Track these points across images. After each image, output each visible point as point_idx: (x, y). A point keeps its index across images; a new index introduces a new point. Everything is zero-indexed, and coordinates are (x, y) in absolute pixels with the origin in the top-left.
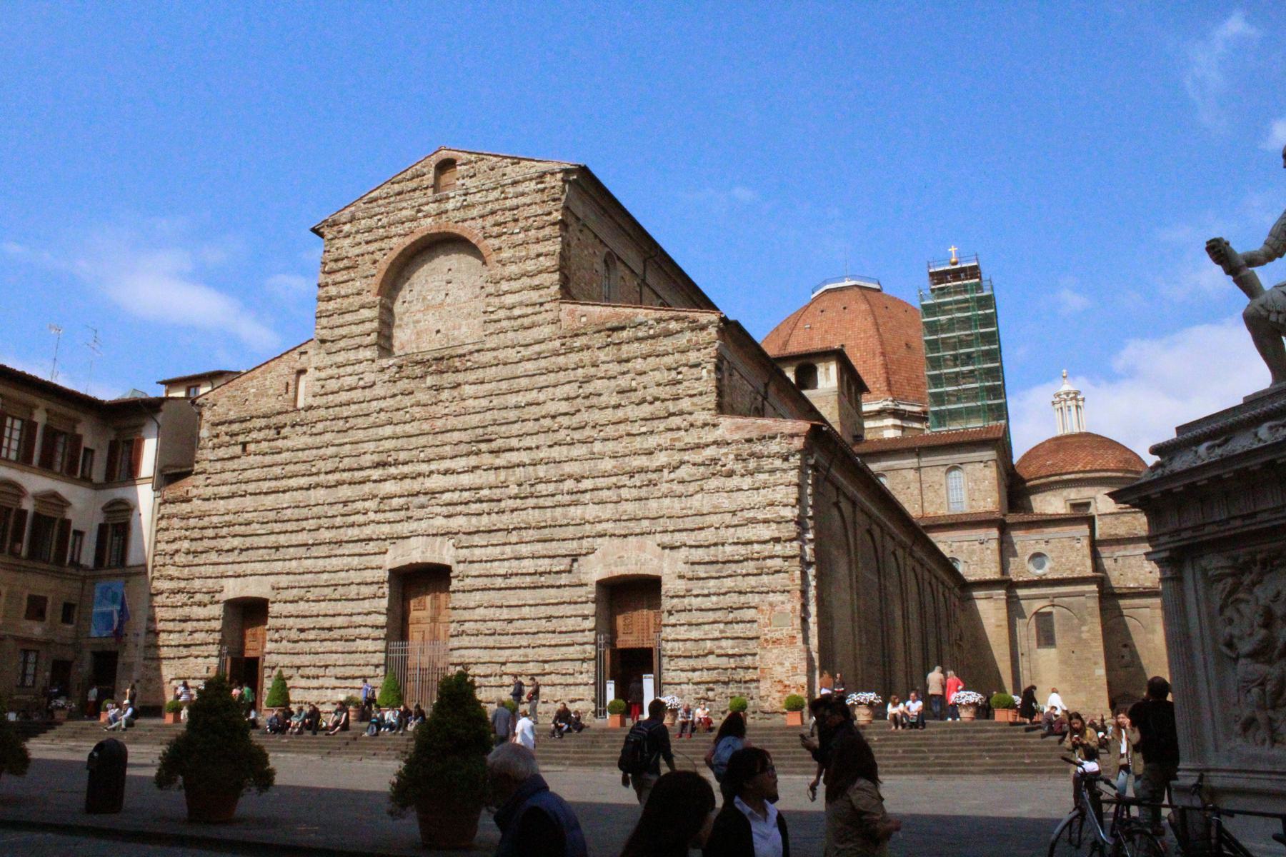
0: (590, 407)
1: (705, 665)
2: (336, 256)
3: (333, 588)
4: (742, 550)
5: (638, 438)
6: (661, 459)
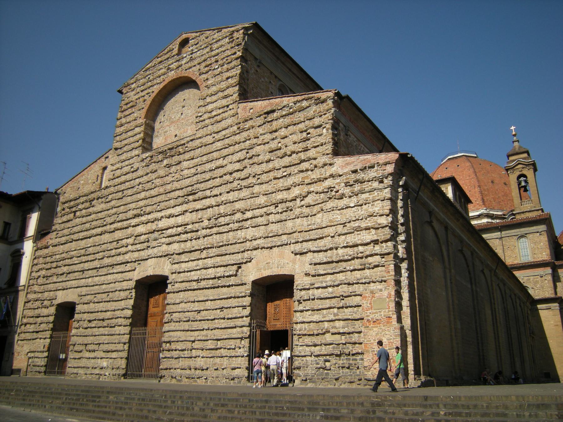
0: (252, 164)
1: (323, 342)
2: (127, 101)
3: (108, 294)
4: (350, 251)
5: (281, 180)
6: (296, 191)
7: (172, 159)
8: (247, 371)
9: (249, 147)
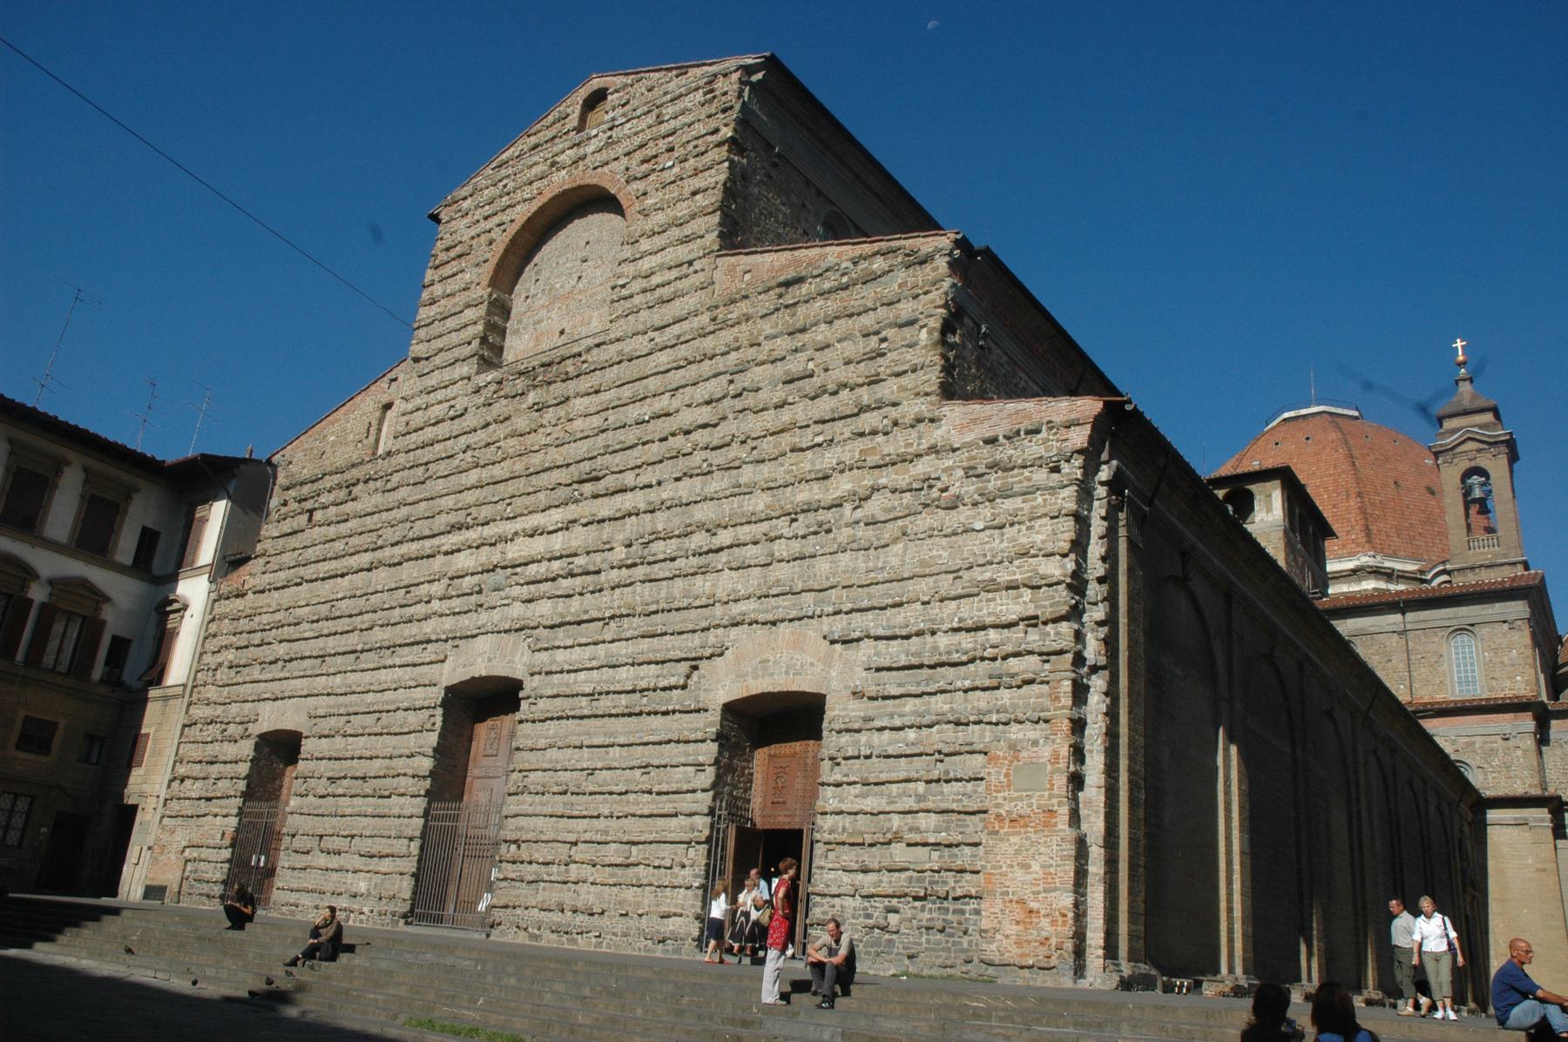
0: (741, 412)
2: (448, 241)
4: (966, 641)
5: (809, 454)
6: (843, 485)
7: (548, 391)
8: (697, 924)
9: (736, 369)
